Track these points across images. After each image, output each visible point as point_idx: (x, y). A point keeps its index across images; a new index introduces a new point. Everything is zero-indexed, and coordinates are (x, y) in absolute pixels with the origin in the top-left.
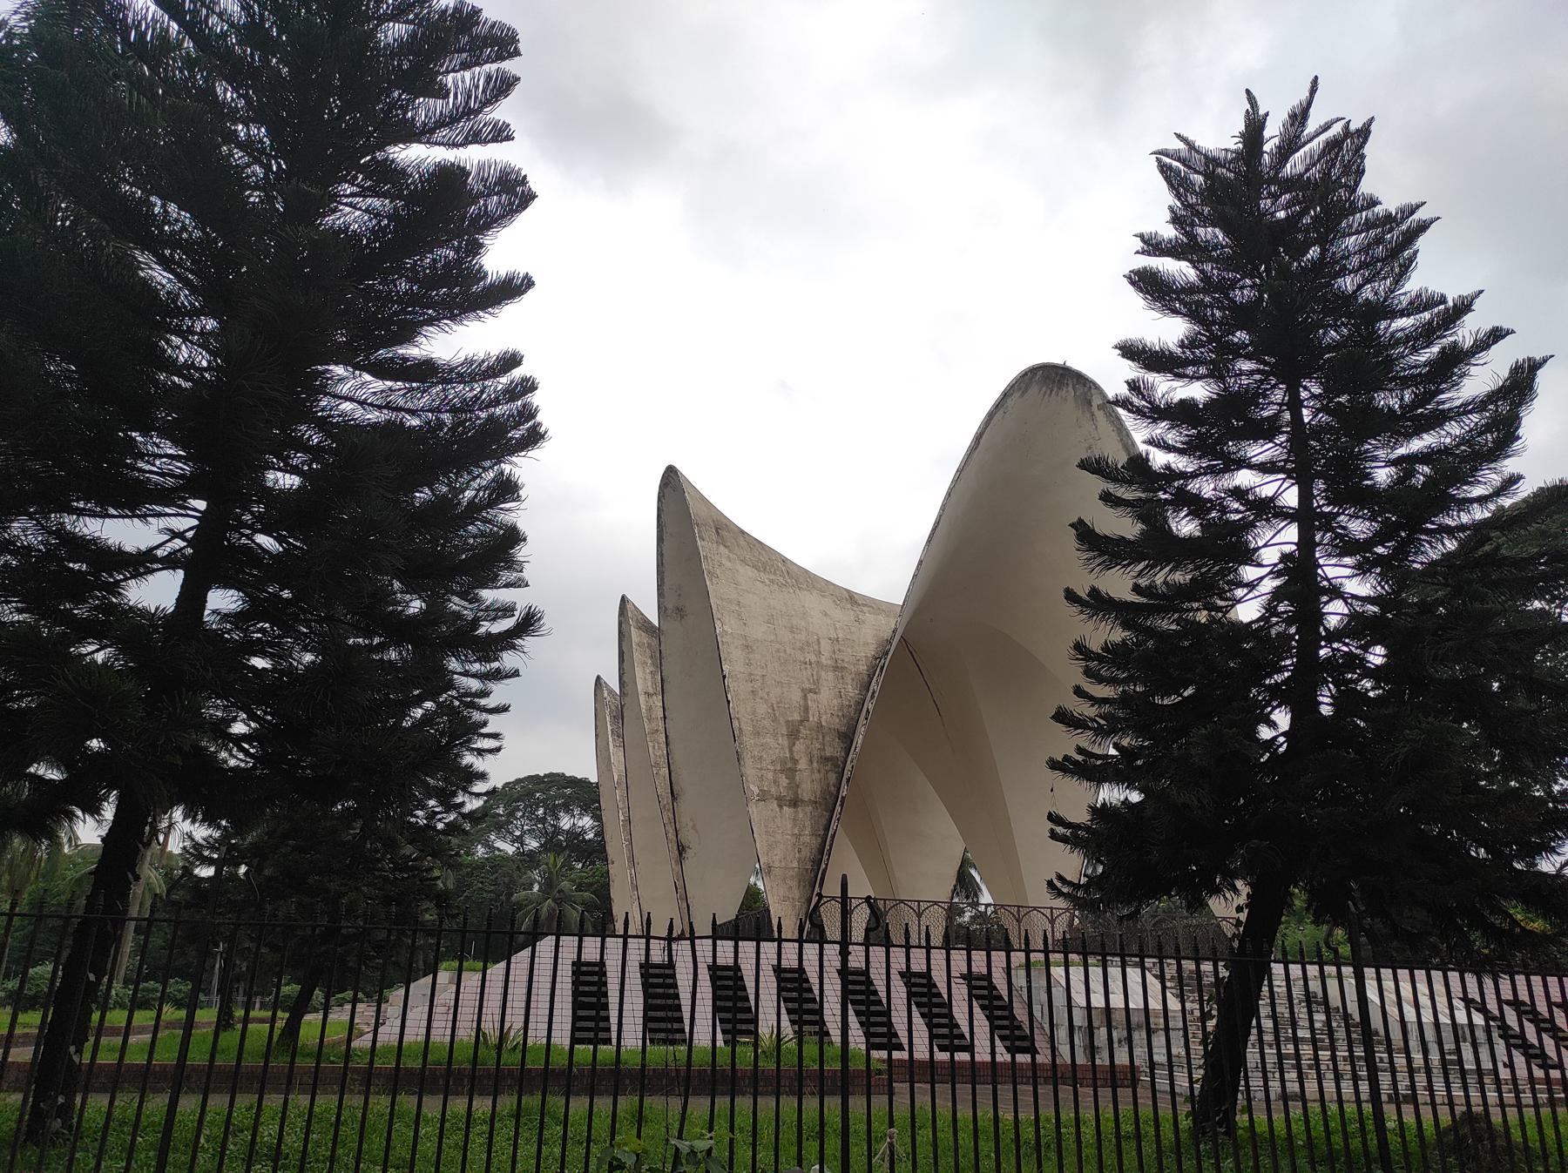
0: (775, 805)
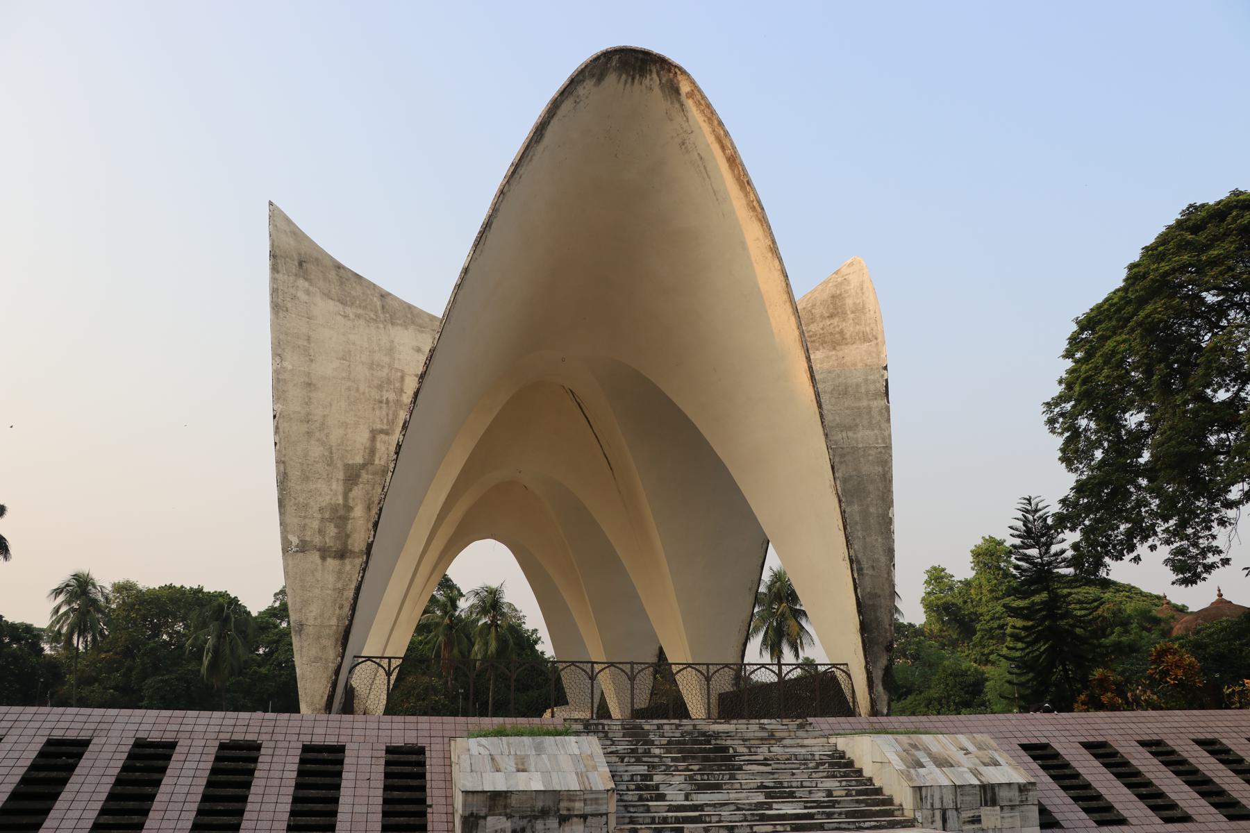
0: (315, 557)
